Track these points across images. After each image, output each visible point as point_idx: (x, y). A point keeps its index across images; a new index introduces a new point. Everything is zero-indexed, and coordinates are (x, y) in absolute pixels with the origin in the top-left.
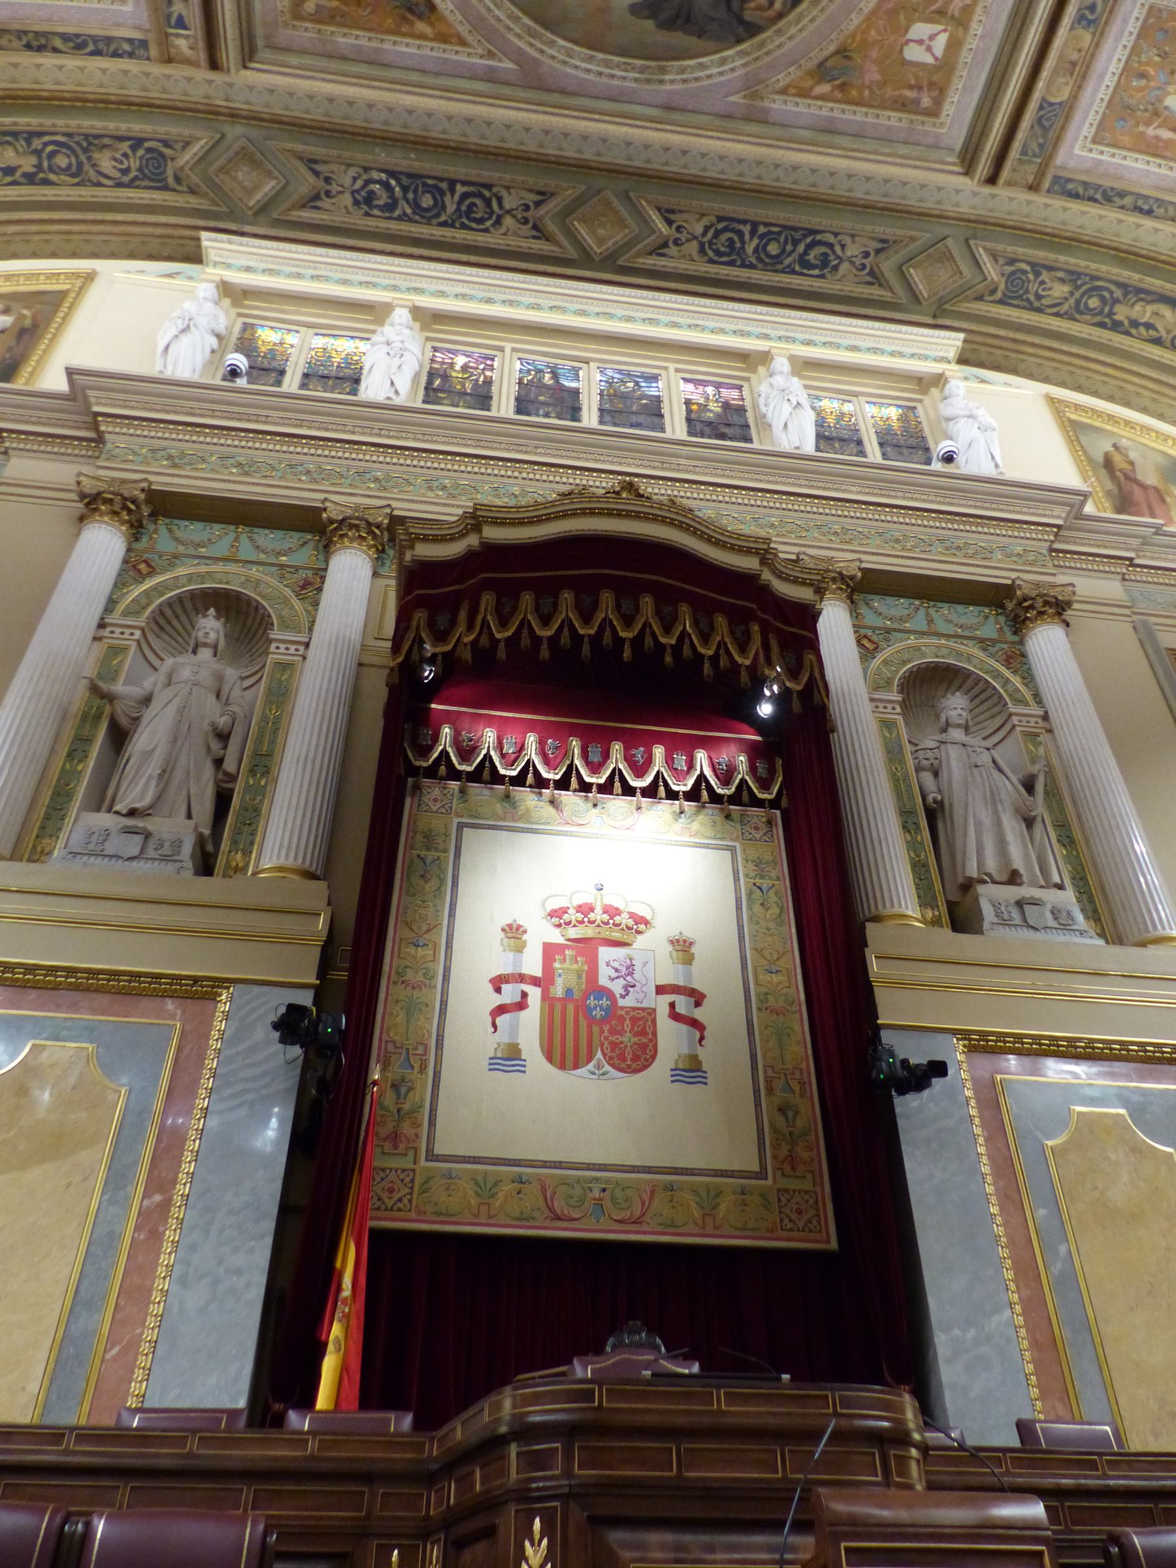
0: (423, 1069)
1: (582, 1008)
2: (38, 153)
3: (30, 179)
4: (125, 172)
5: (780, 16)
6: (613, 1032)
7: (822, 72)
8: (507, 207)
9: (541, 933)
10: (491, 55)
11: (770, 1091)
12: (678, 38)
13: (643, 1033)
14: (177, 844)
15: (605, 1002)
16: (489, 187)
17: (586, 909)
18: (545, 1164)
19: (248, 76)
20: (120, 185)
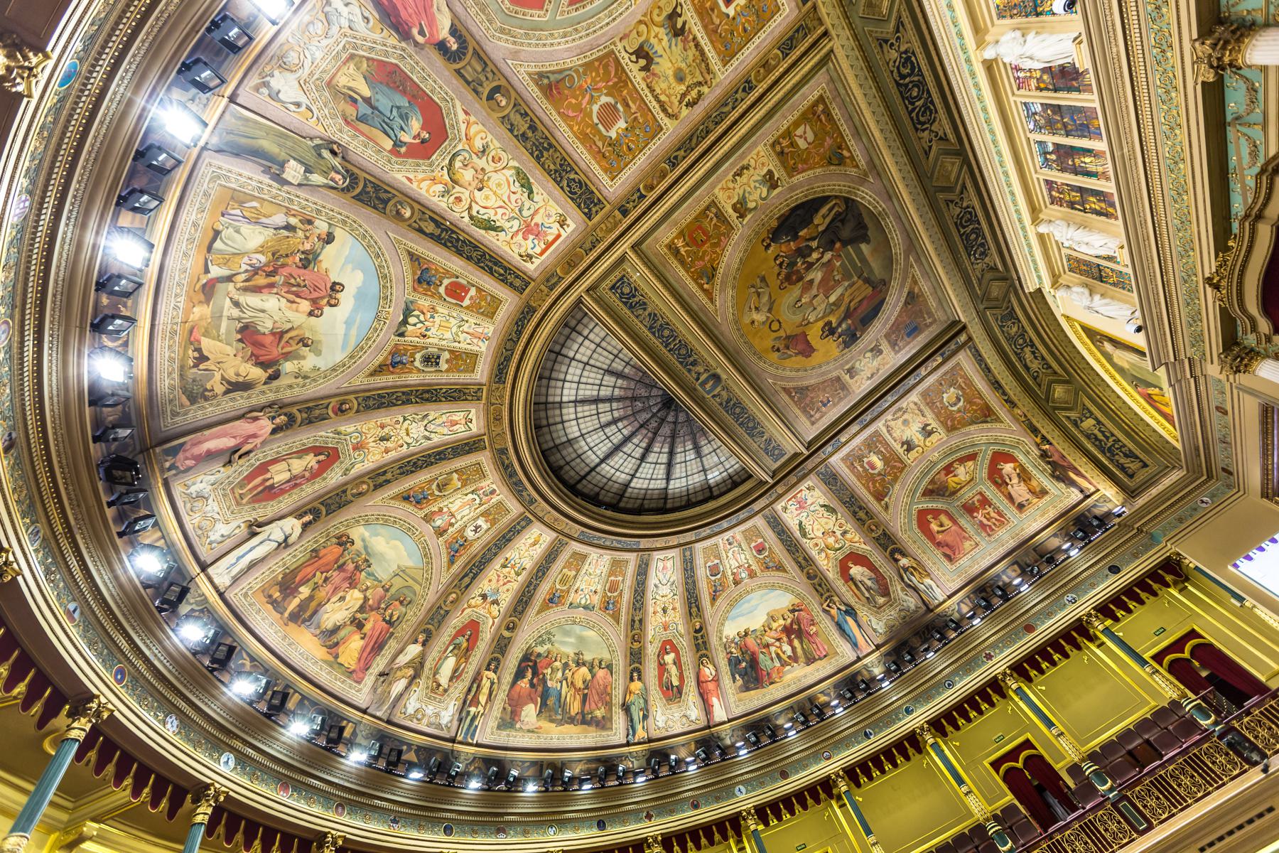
2: (1022, 349)
3: (1033, 345)
4: (1014, 323)
5: (836, 197)
7: (841, 161)
8: (959, 210)
10: (912, 266)
12: (867, 220)
16: (956, 223)
19: (963, 320)
20: (1019, 321)
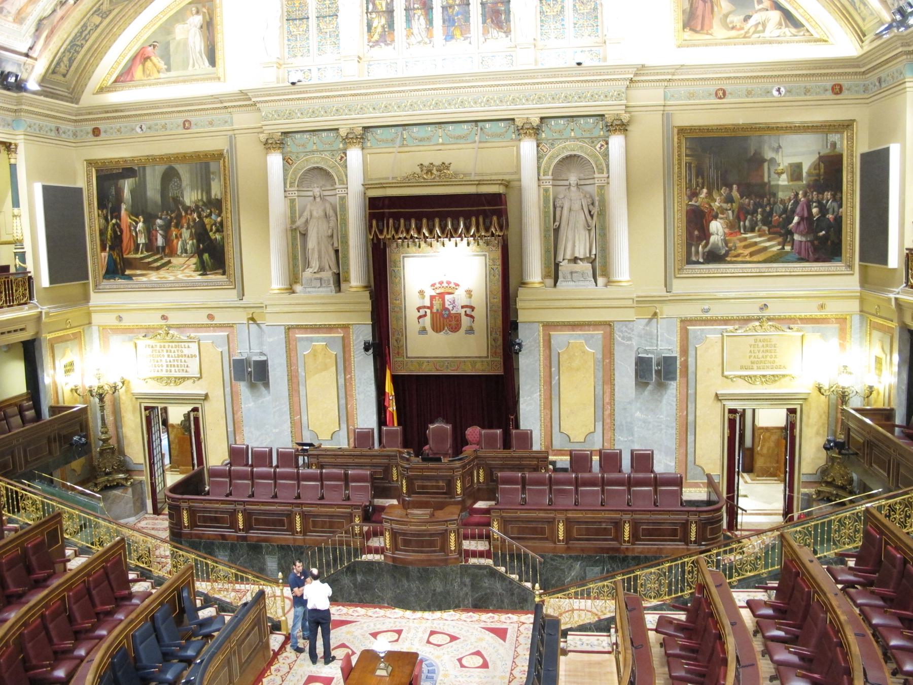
0: (402, 335)
1: (442, 315)
6: (450, 321)
9: (430, 292)
11: (491, 335)
13: (457, 321)
14: (329, 280)
15: (447, 312)
17: (441, 283)
18: (434, 358)
